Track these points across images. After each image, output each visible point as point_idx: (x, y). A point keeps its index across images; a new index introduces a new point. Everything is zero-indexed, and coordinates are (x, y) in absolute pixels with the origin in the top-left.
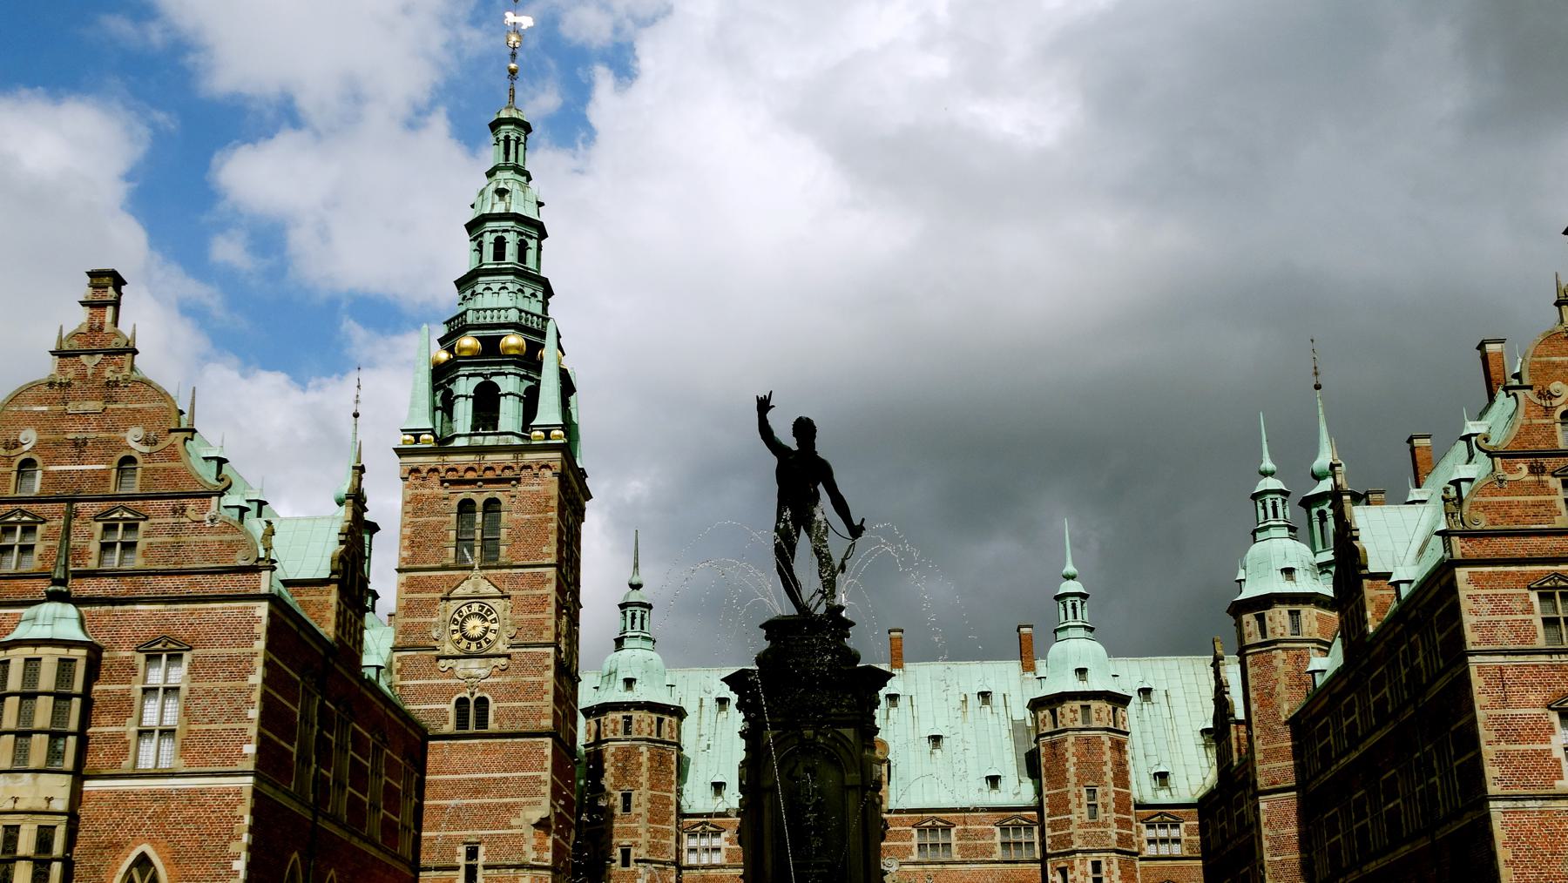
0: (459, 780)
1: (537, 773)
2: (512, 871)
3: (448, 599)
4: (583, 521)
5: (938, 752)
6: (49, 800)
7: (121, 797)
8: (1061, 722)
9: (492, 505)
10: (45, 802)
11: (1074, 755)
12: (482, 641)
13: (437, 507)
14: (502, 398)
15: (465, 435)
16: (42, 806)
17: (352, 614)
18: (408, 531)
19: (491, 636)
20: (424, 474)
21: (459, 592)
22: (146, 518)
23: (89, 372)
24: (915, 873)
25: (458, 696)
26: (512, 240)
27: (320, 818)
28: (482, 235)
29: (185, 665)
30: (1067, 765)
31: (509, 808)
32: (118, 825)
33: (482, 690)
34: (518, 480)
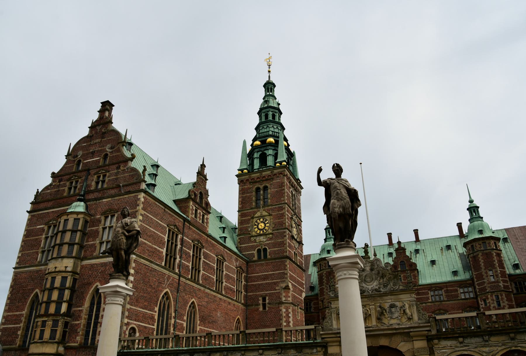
0: (259, 275)
1: (284, 271)
2: (277, 305)
3: (253, 218)
4: (301, 195)
5: (435, 266)
6: (66, 267)
7: (92, 265)
8: (476, 249)
9: (266, 188)
10: (65, 268)
11: (482, 259)
12: (264, 230)
13: (249, 191)
14: (268, 157)
15: (257, 169)
16: (63, 269)
17: (201, 212)
18: (241, 199)
19: (266, 228)
20: (245, 182)
21: (256, 215)
22: (109, 171)
23: (98, 131)
24: (431, 305)
25: (257, 248)
26: (270, 114)
27: (181, 278)
28: (261, 114)
29: (115, 218)
30: (480, 263)
31: (275, 283)
32: (90, 276)
33: (265, 246)
34: (272, 179)
